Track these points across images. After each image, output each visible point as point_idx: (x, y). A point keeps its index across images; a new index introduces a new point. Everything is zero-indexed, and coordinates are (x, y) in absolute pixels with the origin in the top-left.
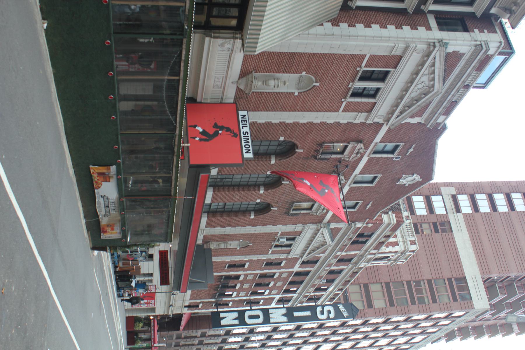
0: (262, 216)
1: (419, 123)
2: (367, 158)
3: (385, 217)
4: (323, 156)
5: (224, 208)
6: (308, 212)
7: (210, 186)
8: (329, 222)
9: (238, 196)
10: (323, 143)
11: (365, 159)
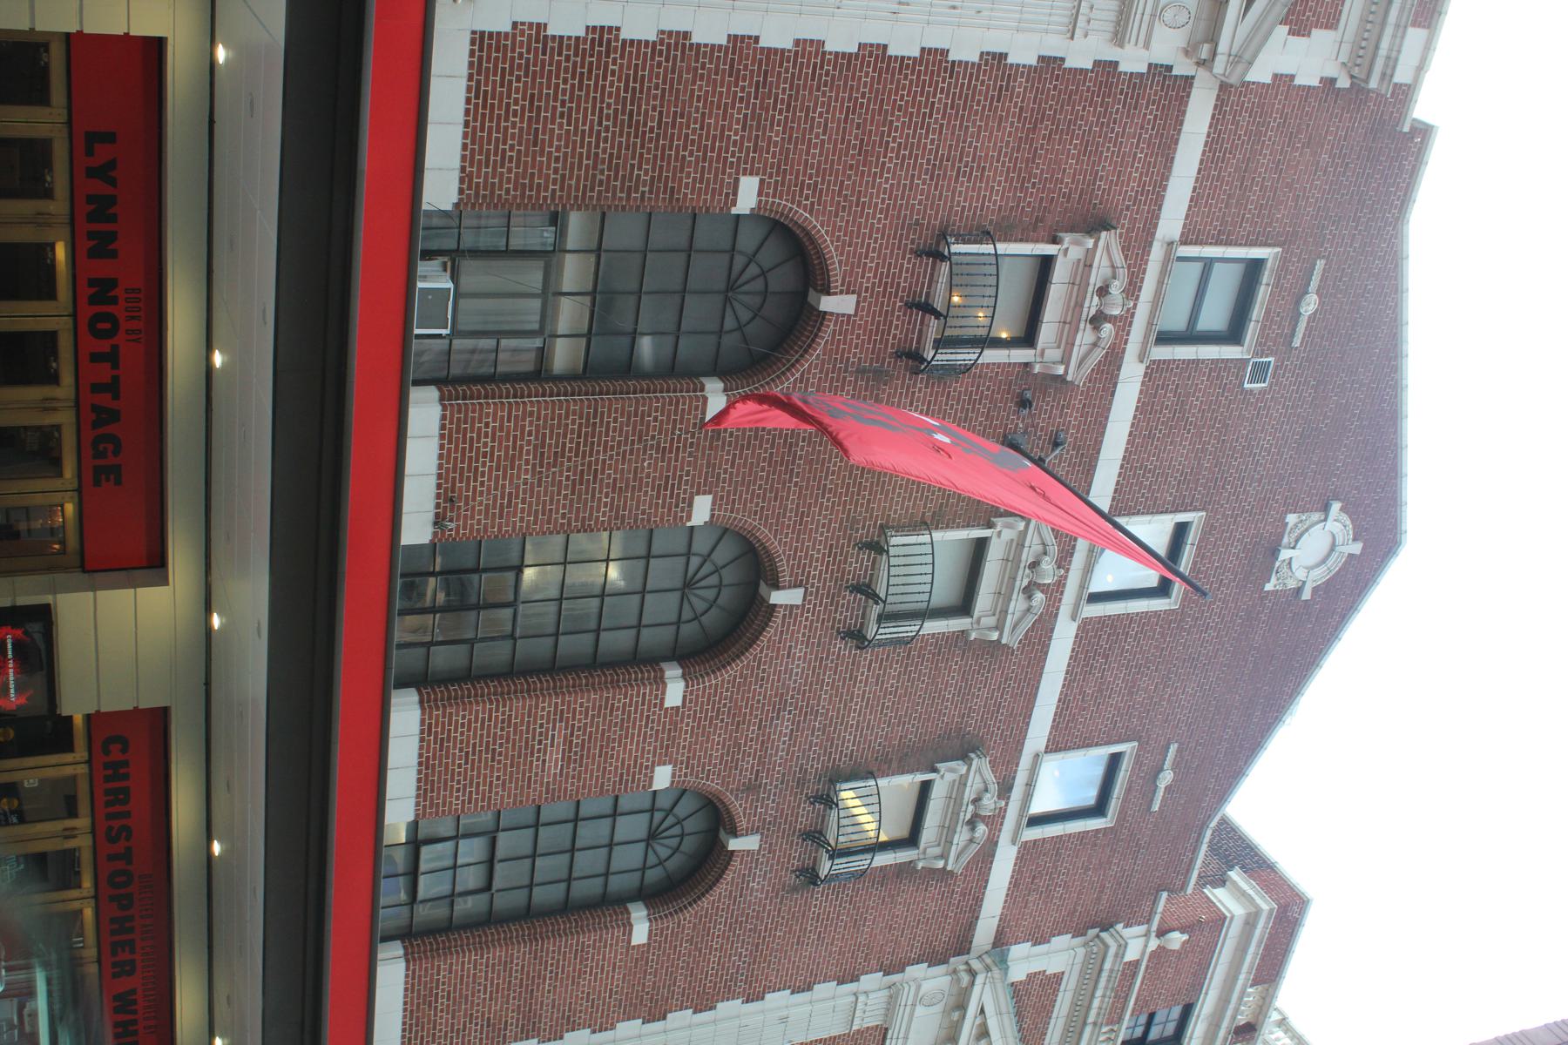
0: (688, 915)
1: (1329, 82)
2: (1141, 369)
3: (1221, 897)
4: (945, 357)
5: (488, 887)
6: (903, 856)
7: (402, 684)
8: (1001, 941)
9: (559, 733)
10: (943, 236)
11: (1131, 377)
